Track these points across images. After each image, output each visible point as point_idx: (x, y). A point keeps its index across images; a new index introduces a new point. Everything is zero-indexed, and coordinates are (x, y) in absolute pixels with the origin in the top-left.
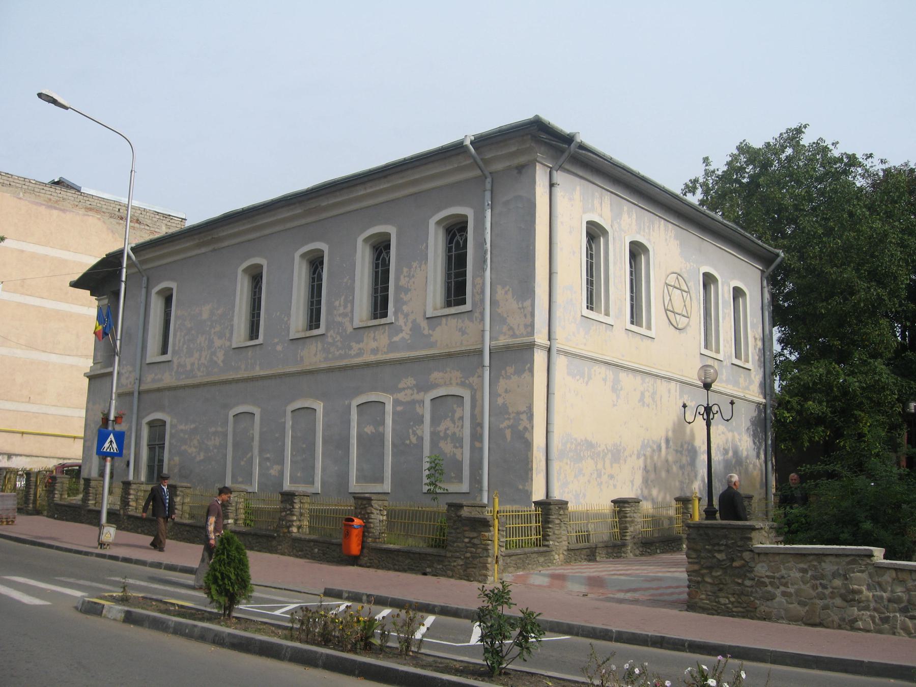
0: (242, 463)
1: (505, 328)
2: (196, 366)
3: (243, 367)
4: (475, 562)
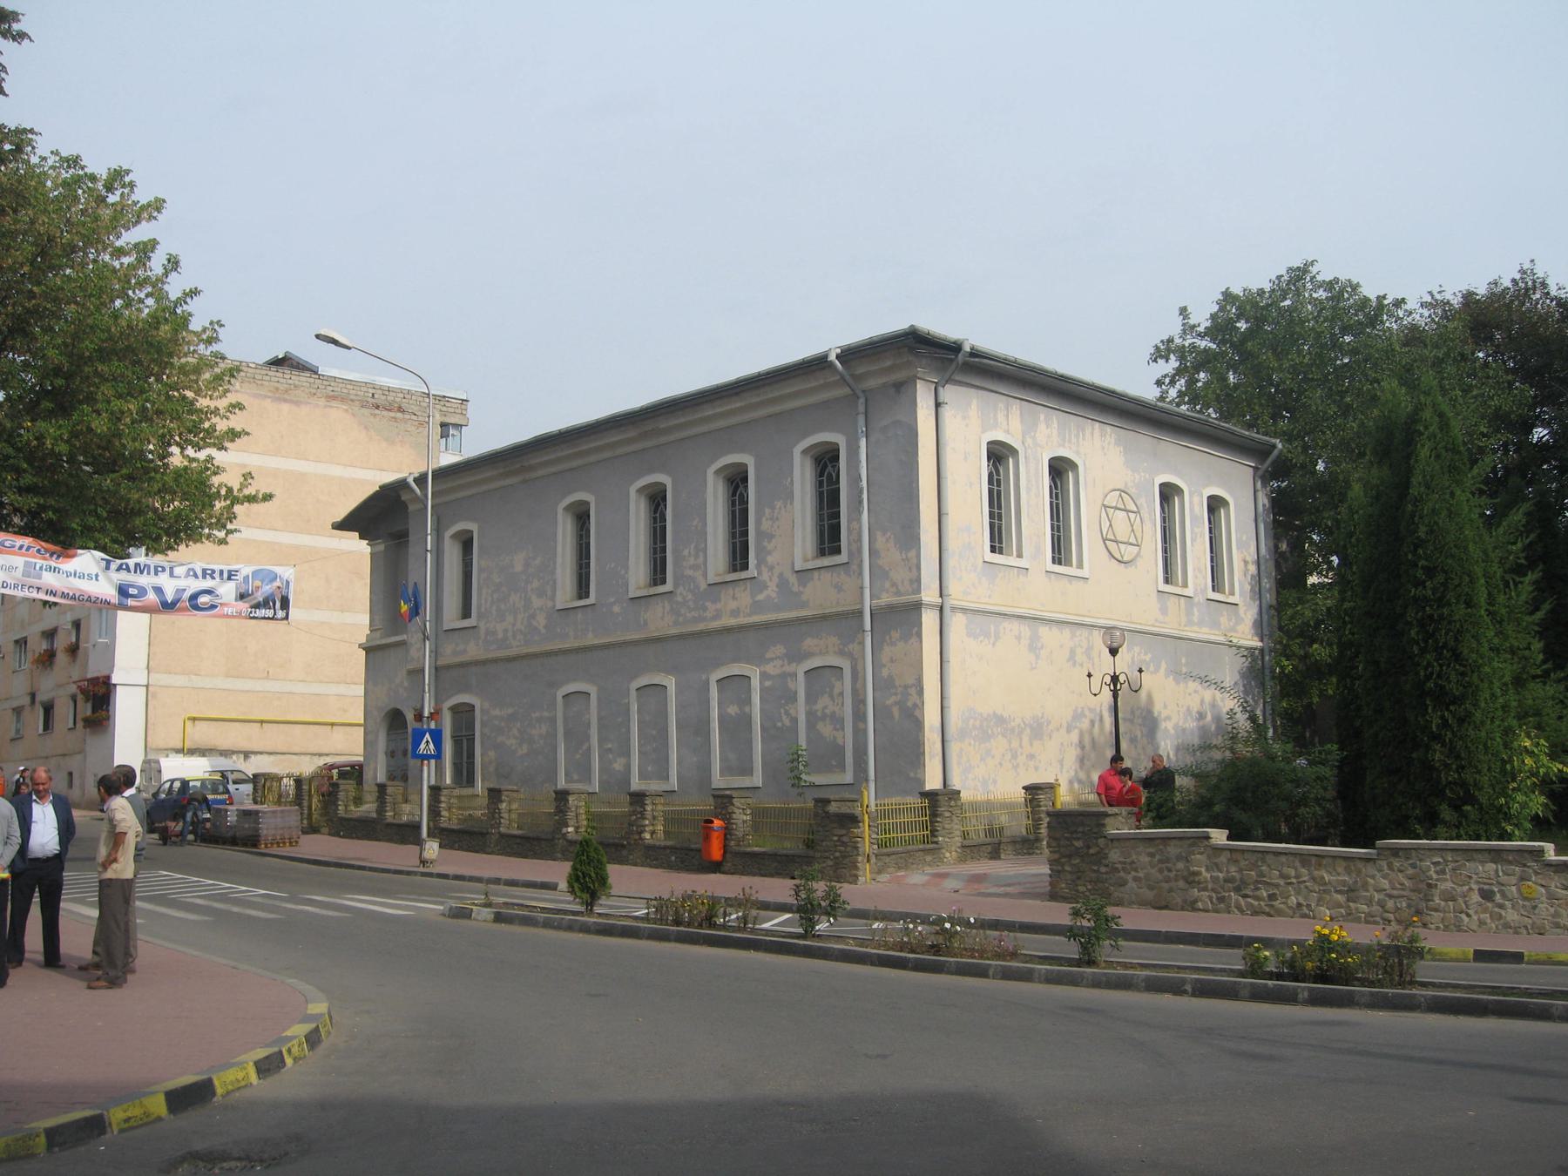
2: (510, 634)
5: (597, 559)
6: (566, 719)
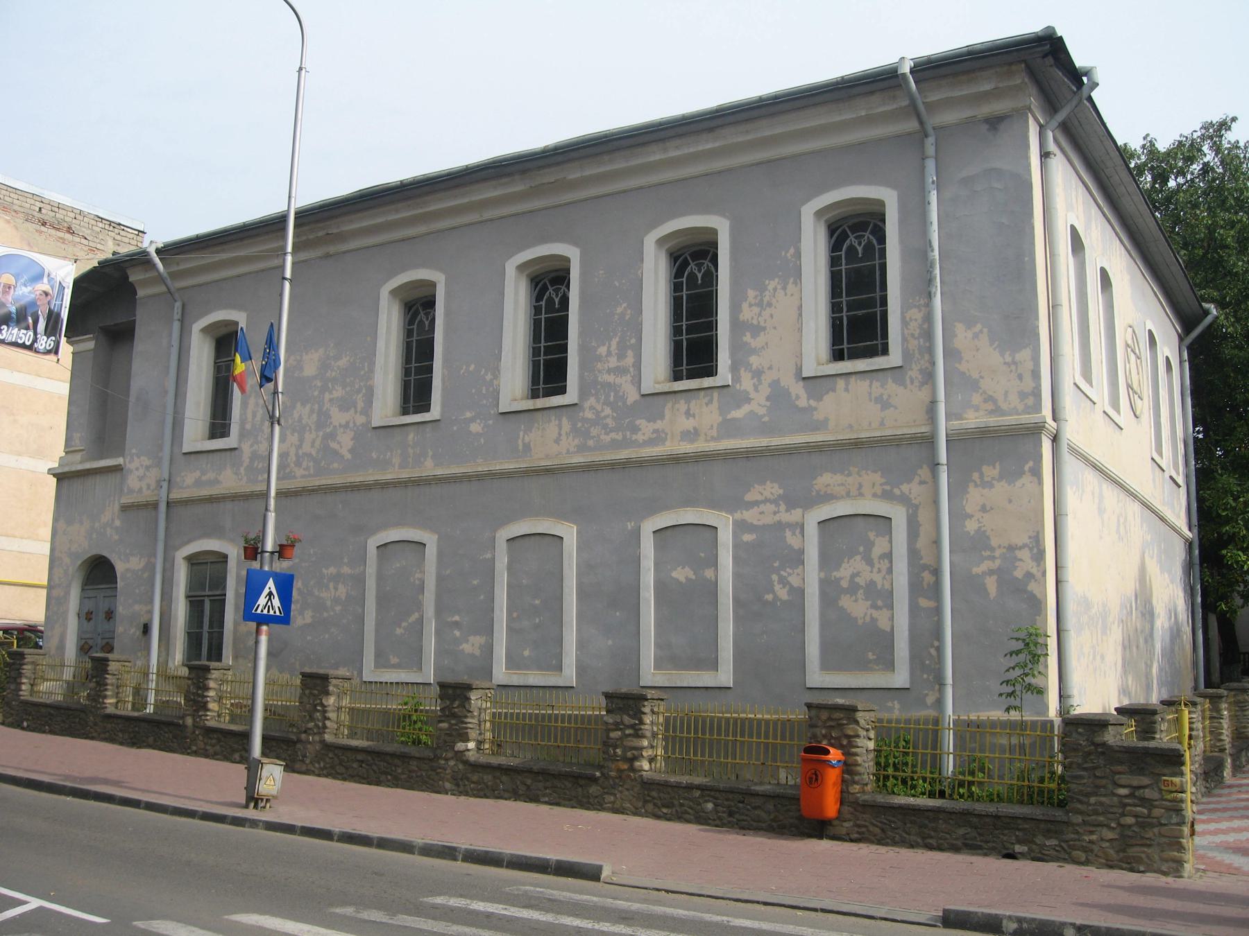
0: (399, 631)
1: (976, 399)
3: (396, 461)
4: (1150, 835)
5: (446, 360)
6: (380, 578)
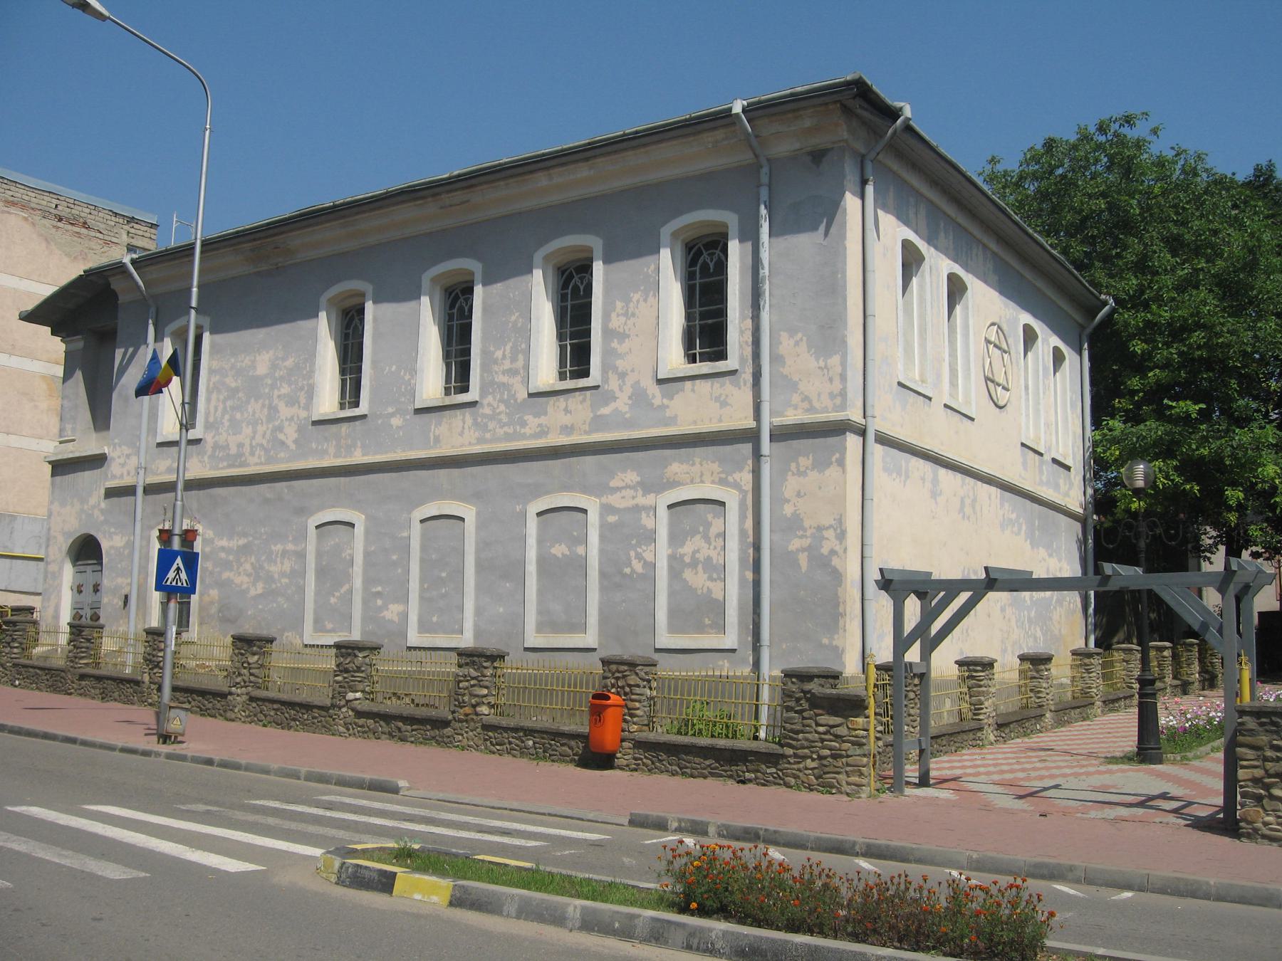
0: (333, 600)
1: (796, 398)
2: (247, 449)
3: (332, 450)
5: (374, 363)
6: (319, 555)
